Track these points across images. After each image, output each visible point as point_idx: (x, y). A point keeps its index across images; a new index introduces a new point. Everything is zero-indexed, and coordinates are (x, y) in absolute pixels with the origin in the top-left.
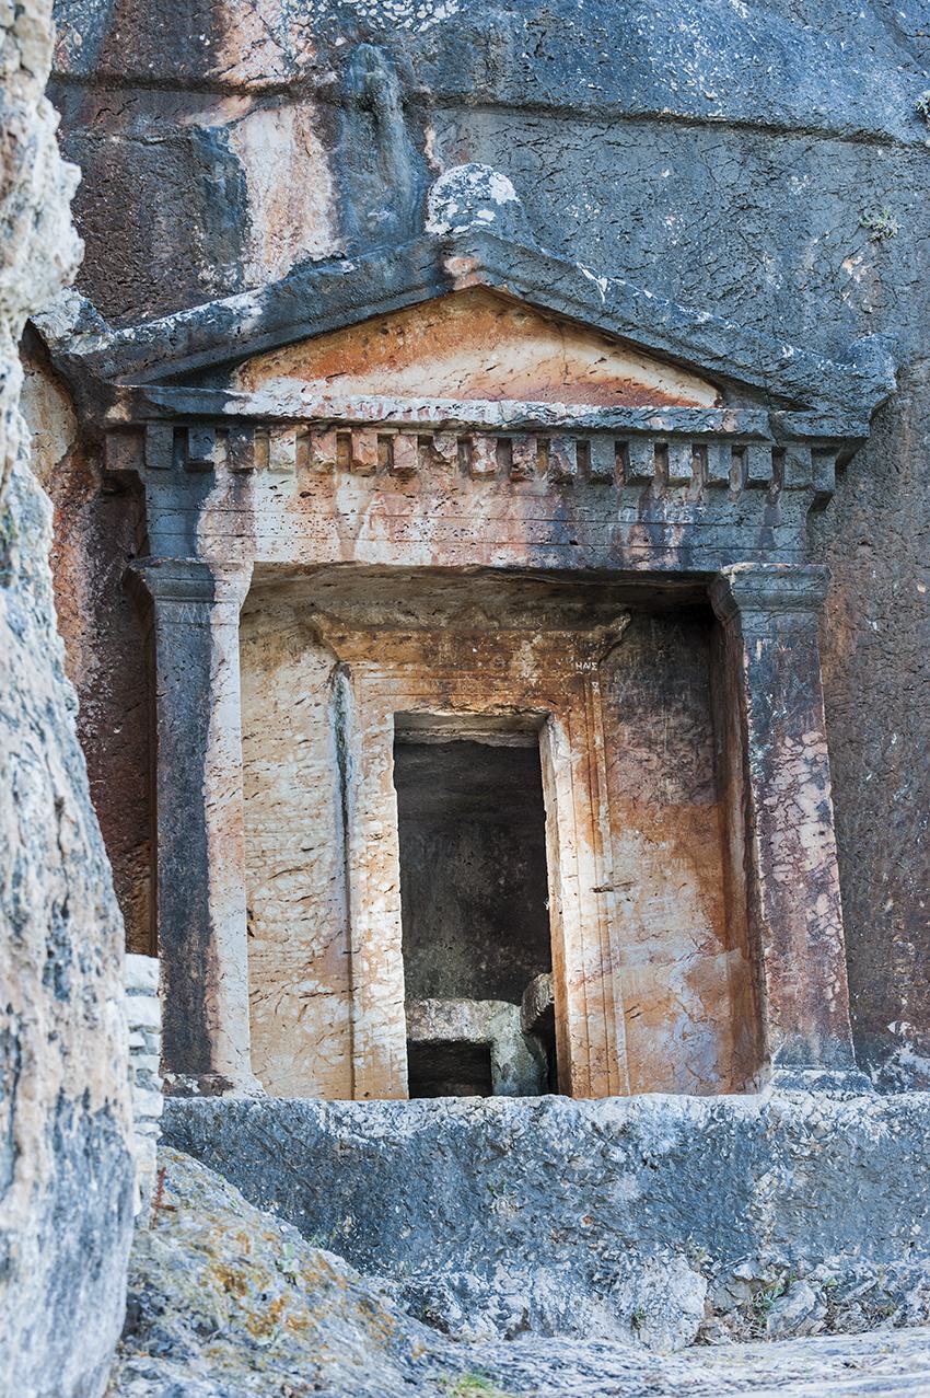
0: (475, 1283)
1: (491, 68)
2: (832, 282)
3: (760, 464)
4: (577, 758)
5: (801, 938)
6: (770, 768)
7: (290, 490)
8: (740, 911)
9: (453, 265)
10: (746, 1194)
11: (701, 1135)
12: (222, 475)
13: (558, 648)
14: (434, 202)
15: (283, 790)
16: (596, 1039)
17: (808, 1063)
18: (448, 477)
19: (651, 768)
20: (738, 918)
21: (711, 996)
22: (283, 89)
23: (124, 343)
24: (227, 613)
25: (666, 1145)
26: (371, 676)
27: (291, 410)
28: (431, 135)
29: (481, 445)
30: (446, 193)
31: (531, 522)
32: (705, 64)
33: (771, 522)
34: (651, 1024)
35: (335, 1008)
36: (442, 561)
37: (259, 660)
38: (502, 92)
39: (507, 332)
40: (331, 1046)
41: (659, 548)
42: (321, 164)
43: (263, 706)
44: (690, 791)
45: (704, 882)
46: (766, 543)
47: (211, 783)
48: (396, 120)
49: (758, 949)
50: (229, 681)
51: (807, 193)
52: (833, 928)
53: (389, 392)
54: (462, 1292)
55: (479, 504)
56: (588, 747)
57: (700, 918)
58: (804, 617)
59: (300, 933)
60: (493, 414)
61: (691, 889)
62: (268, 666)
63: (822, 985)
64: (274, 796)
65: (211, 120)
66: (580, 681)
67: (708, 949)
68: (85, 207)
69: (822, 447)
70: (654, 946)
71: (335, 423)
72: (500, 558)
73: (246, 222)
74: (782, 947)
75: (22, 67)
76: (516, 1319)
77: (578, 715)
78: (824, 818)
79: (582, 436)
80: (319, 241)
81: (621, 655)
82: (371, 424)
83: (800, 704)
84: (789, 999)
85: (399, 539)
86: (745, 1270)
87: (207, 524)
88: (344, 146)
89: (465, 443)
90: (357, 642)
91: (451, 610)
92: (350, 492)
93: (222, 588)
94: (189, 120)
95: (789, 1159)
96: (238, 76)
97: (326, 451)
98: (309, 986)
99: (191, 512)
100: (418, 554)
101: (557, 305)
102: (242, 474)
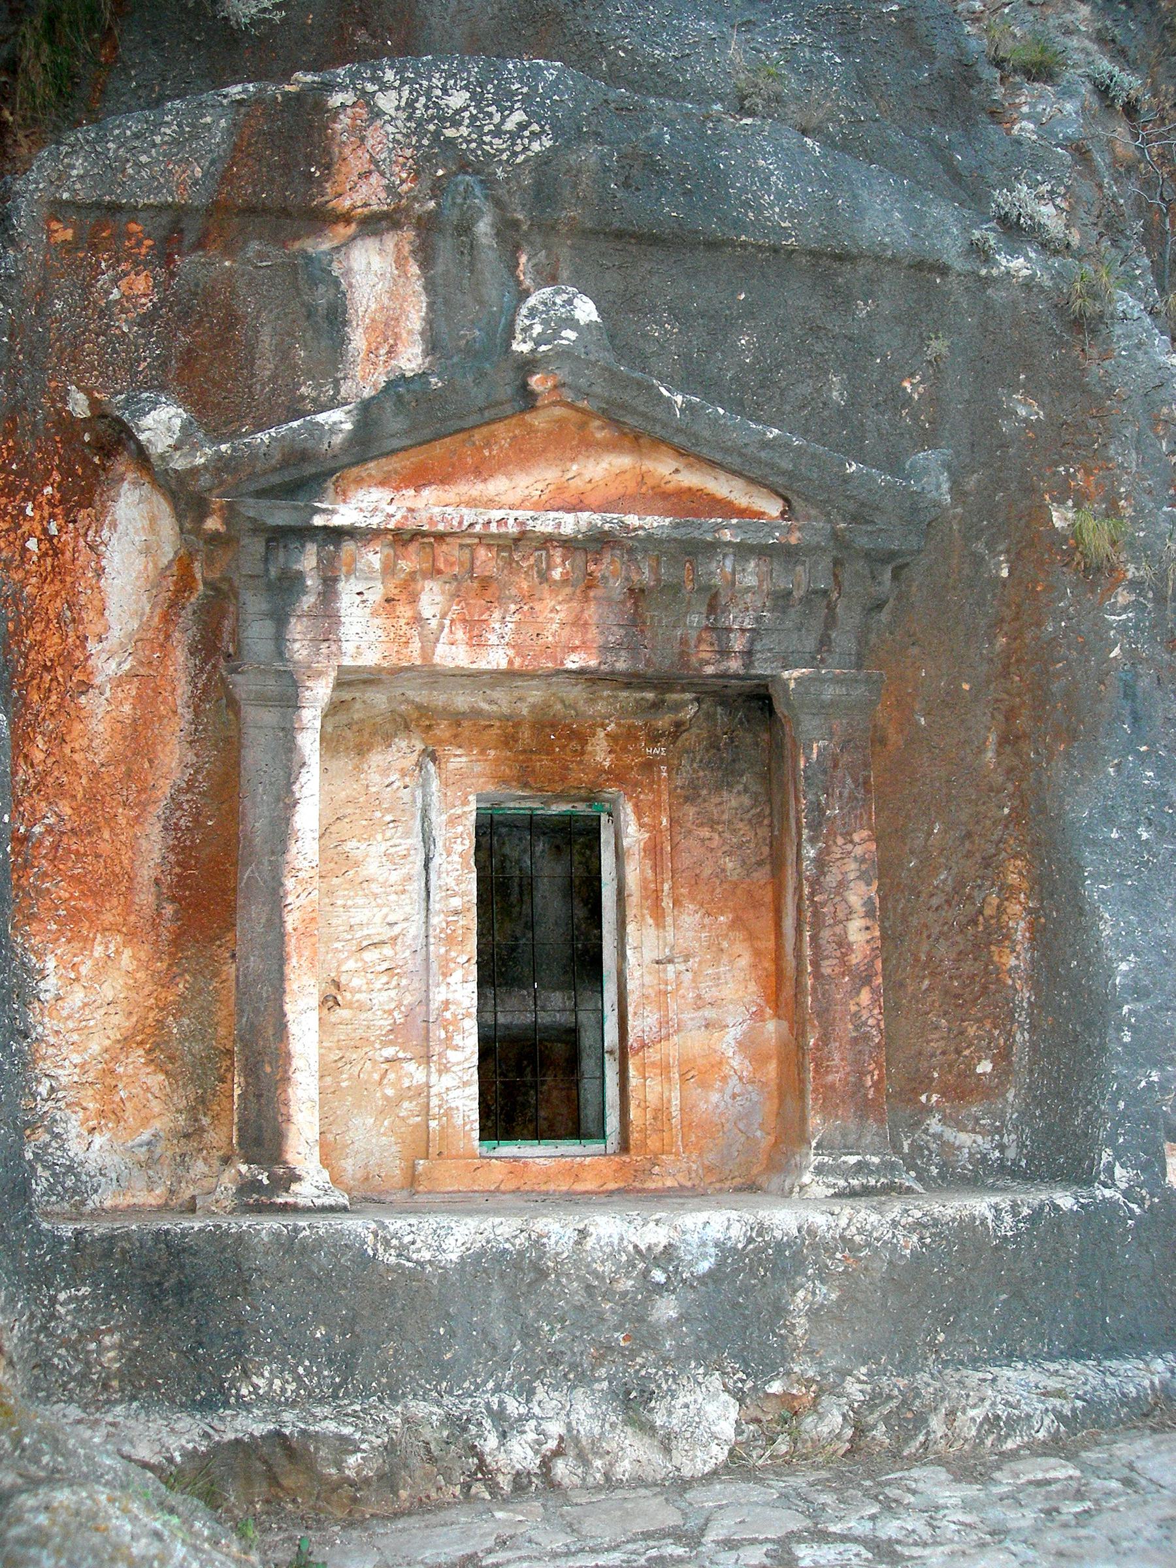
0: (513, 1407)
6: (821, 863)
7: (376, 595)
8: (788, 991)
9: (536, 382)
10: (780, 1310)
14: (521, 322)
15: (371, 868)
16: (652, 1098)
21: (758, 1058)
23: (220, 456)
24: (311, 716)
25: (704, 1266)
27: (374, 522)
28: (523, 259)
31: (603, 629)
32: (781, 196)
33: (831, 621)
42: (418, 286)
45: (757, 953)
46: (825, 642)
47: (289, 883)
50: (310, 786)
52: (873, 1019)
53: (472, 503)
54: (498, 1415)
56: (654, 828)
57: (752, 987)
61: (744, 962)
66: (649, 766)
67: (758, 1016)
69: (877, 558)
71: (417, 534)
72: (574, 662)
74: (825, 1039)
76: (552, 1444)
78: (869, 914)
85: (477, 642)
87: (298, 632)
88: (440, 268)
94: (297, 245)
95: (823, 1275)
98: (389, 1052)
99: (280, 619)
100: (497, 659)
102: (329, 584)
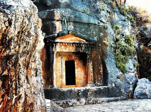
0: (70, 101)
1: (72, 19)
2: (93, 34)
3: (88, 46)
4: (76, 63)
5: (90, 76)
6: (89, 65)
7: (59, 47)
8: (86, 73)
9: (69, 32)
10: (88, 94)
11: (85, 90)
12: (54, 46)
13: (75, 56)
14: (68, 28)
15: (58, 65)
16: (77, 81)
17: (91, 84)
18: (69, 46)
19: (81, 64)
20: (86, 74)
21: (84, 78)
22: (58, 20)
23: (48, 37)
24: (55, 55)
25: (83, 91)
26: (64, 58)
27: (59, 42)
28: (68, 23)
29: (71, 44)
30: (69, 27)
31: (74, 49)
32: (85, 19)
33: (89, 49)
34: (81, 80)
35: (61, 79)
36: (69, 51)
37: (57, 57)
38: (73, 21)
39: (73, 36)
40: (61, 82)
41: (82, 51)
42: (61, 25)
43: (57, 60)
44: (83, 65)
45: (84, 71)
46: (89, 50)
47: (54, 66)
48: (66, 22)
49: (88, 76)
50: (55, 59)
51: (91, 28)
52: (92, 75)
53: (65, 40)
54: (69, 101)
55: (71, 48)
56: (77, 63)
57: (84, 73)
58: (91, 55)
59: (59, 75)
60: (72, 42)
61: (83, 72)
62: (57, 57)
63: (92, 79)
64: (57, 66)
65: (54, 22)
66: (77, 58)
67: (84, 75)
68: (45, 40)
69: (92, 44)
70: (81, 75)
71: (62, 42)
72: (72, 51)
73: (56, 29)
74: (89, 76)
75: (38, 27)
76: (73, 103)
77: (76, 61)
78: (92, 68)
79: (77, 43)
80: (61, 30)
81: (79, 57)
82: (64, 43)
83: (90, 61)
84: (90, 80)
85: (66, 50)
86: (87, 99)
87: (54, 49)
88: (62, 24)
89: (70, 44)
90: (63, 56)
91: (69, 54)
92: (63, 47)
93: (54, 53)
94: (52, 22)
95: (90, 91)
96: (56, 19)
97: (61, 44)
98: (59, 78)
99: (52, 48)
100: (67, 51)
101: (76, 35)
102: (56, 46)
